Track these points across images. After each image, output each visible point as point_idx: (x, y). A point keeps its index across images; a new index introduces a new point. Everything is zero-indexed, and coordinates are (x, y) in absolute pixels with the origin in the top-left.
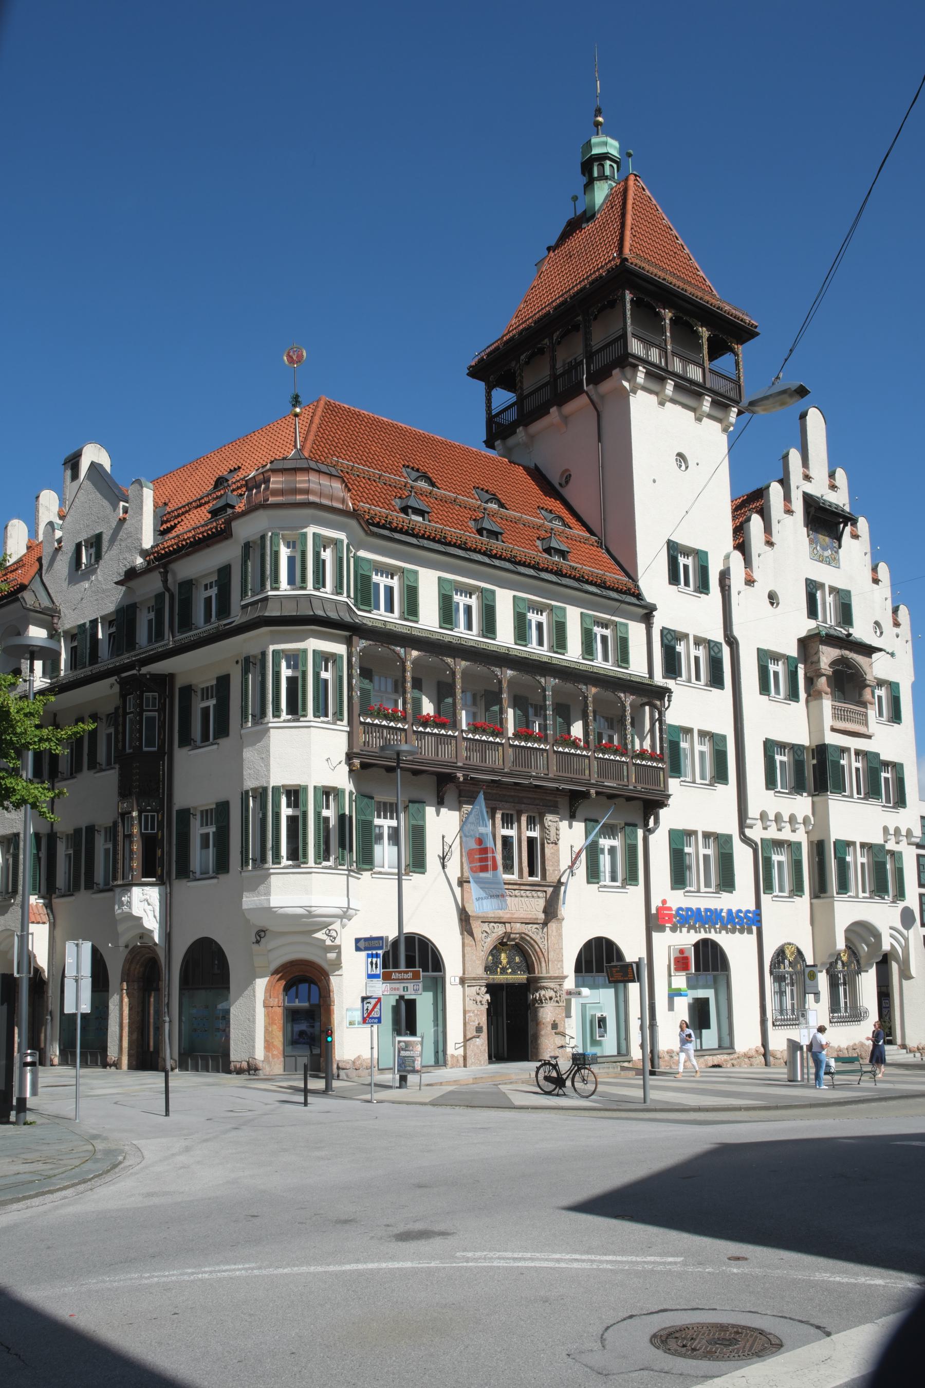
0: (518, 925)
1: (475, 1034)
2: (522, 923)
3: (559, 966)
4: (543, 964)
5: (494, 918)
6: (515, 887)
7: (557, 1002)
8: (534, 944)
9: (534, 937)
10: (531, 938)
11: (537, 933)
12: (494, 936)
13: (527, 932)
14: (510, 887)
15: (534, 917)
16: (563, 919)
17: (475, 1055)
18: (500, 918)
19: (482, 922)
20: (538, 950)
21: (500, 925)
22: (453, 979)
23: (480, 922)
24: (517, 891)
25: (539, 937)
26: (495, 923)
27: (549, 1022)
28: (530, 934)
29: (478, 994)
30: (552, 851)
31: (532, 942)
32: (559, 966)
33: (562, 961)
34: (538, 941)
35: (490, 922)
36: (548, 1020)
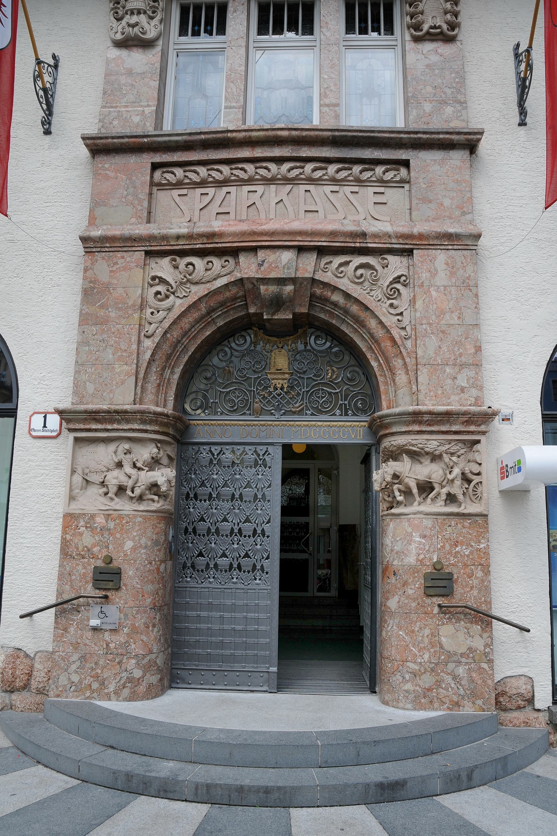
0: (287, 256)
1: (89, 590)
2: (301, 249)
3: (462, 381)
4: (401, 378)
5: (190, 237)
6: (277, 152)
7: (451, 498)
8: (363, 315)
9: (356, 291)
10: (347, 296)
11: (375, 282)
12: (199, 291)
13: (327, 277)
14: (259, 152)
15: (351, 228)
16: (478, 236)
17: (83, 658)
18: (211, 236)
19: (149, 254)
20: (380, 333)
21: (217, 263)
22: (38, 421)
23: (141, 255)
24: (286, 166)
25: (378, 293)
26: (201, 253)
27: (413, 570)
28: (344, 284)
29: (119, 465)
30: (434, 58)
31: (354, 309)
32: (462, 381)
33: (478, 365)
34: (372, 306)
35: (183, 253)
36: (411, 560)
